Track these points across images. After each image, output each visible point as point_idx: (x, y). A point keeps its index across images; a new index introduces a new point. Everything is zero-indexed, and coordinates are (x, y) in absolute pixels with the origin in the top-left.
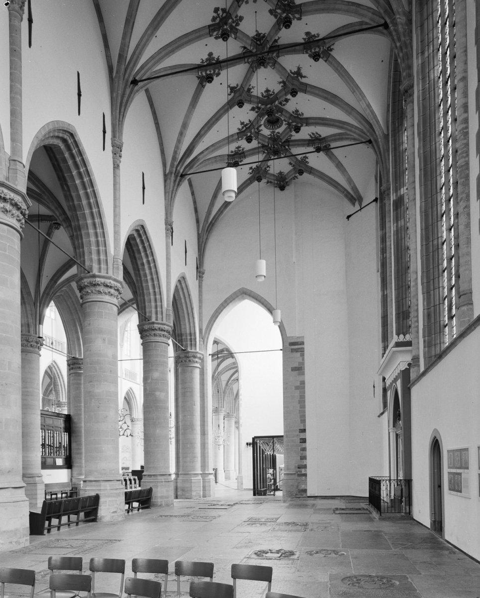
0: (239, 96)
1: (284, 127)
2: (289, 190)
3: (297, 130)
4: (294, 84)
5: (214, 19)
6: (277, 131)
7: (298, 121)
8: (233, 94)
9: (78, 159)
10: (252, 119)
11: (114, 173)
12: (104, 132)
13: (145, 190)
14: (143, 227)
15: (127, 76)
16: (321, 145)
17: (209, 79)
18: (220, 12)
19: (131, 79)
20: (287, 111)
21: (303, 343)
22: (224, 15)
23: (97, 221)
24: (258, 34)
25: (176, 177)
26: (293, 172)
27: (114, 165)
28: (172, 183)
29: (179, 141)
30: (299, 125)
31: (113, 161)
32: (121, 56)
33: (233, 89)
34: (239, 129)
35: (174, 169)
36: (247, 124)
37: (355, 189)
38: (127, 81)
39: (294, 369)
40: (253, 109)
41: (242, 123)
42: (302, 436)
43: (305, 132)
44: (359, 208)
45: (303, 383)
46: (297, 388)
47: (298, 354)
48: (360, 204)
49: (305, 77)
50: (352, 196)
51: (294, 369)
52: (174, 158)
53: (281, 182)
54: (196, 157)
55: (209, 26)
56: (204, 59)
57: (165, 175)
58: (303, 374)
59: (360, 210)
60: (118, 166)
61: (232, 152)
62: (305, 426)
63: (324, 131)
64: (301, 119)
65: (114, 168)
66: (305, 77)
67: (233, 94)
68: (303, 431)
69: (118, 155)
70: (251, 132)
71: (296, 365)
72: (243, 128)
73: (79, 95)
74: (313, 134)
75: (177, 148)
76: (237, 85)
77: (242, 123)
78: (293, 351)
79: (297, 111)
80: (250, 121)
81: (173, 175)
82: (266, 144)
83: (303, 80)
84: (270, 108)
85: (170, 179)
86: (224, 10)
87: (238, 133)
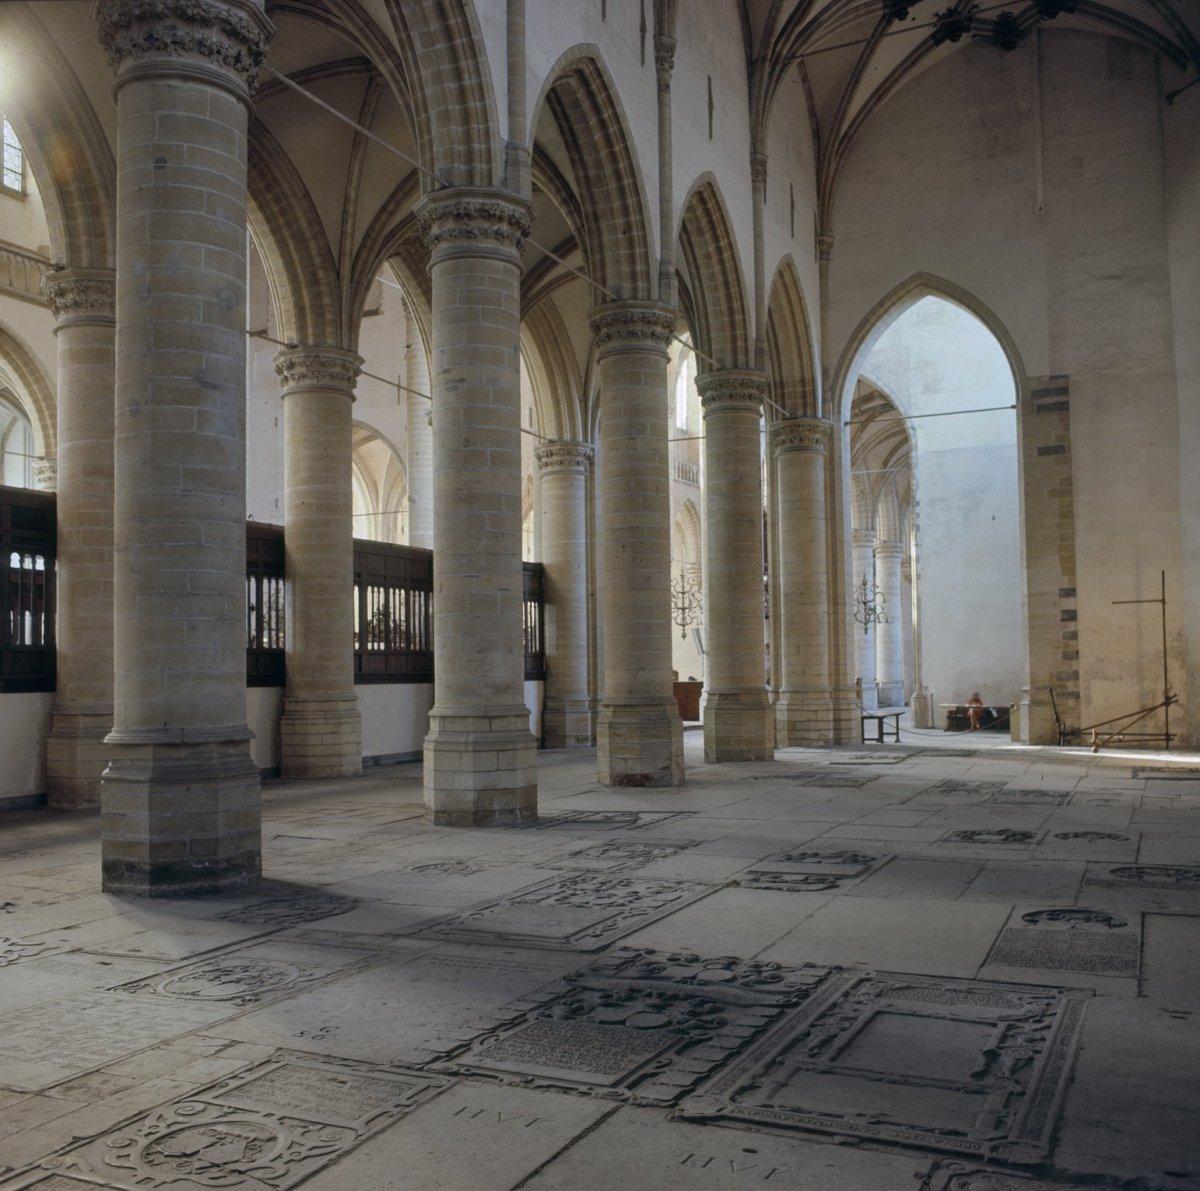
9: (600, 98)
13: (714, 111)
14: (710, 185)
21: (1064, 391)
23: (631, 201)
27: (659, 85)
39: (1044, 451)
42: (1068, 604)
45: (1069, 482)
46: (1053, 493)
47: (1054, 417)
51: (1044, 451)
54: (815, 19)
58: (1068, 462)
60: (668, 86)
62: (1073, 580)
68: (1070, 592)
71: (1052, 442)
78: (1041, 409)
85: (761, 72)
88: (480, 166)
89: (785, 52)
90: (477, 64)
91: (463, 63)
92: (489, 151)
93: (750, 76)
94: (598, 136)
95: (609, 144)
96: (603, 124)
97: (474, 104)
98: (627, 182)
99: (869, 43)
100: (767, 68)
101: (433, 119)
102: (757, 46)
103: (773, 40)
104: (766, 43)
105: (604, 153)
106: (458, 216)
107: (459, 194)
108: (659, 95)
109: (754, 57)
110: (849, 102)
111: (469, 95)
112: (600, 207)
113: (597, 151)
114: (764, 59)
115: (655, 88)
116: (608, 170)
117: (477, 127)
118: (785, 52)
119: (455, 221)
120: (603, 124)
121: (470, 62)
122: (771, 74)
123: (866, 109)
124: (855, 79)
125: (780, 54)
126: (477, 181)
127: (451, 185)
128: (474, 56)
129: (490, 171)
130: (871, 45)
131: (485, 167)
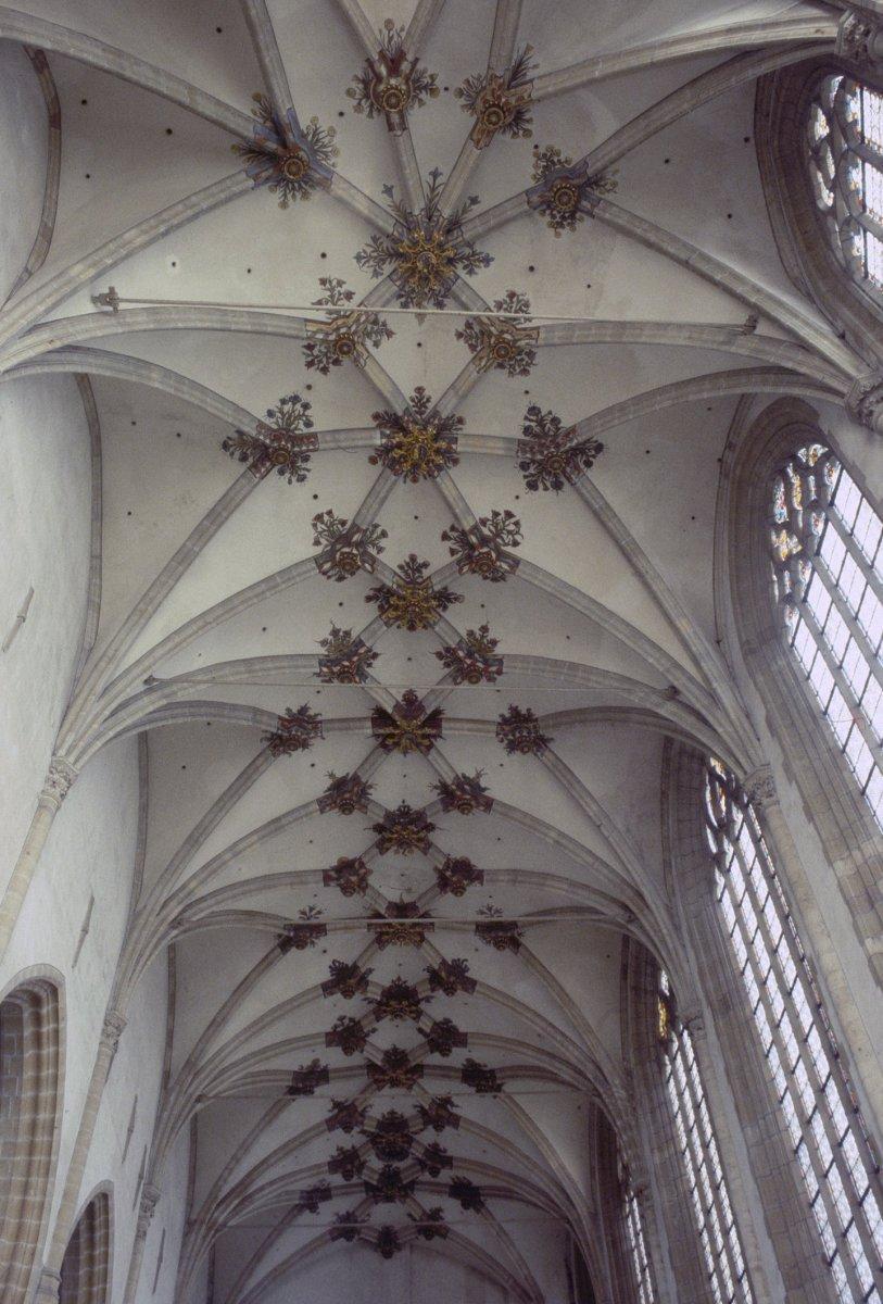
1: (409, 1161)
2: (400, 1257)
3: (435, 1173)
5: (336, 1026)
7: (436, 1158)
8: (336, 1111)
9: (99, 1234)
12: (141, 1177)
15: (194, 1086)
16: (468, 1195)
17: (308, 1091)
18: (346, 1021)
19: (198, 1093)
22: (352, 1024)
26: (413, 1230)
27: (139, 1231)
29: (229, 1169)
30: (439, 1166)
31: (139, 1225)
32: (189, 1064)
33: (337, 1105)
34: (332, 1157)
35: (209, 1216)
36: (348, 1151)
40: (363, 1132)
43: (446, 1176)
49: (457, 1106)
52: (212, 1195)
53: (387, 1243)
55: (327, 1034)
56: (305, 1066)
61: (310, 1186)
63: (477, 1179)
64: (440, 1156)
65: (137, 1236)
66: (457, 1106)
67: (336, 1111)
70: (353, 1166)
72: (339, 1155)
74: (457, 1177)
75: (222, 1179)
76: (346, 1101)
80: (353, 1147)
81: (204, 1227)
82: (375, 1183)
83: (454, 1110)
86: (351, 1020)
87: (329, 1163)
89: (221, 1220)
90: (46, 1183)
91: (33, 1179)
92: (29, 1272)
93: (186, 1235)
95: (90, 1282)
97: (30, 1221)
99: (275, 1229)
100: (203, 1231)
102: (197, 1208)
108: (136, 1240)
109: (194, 1217)
113: (76, 1285)
117: (26, 1245)
121: (41, 1180)
122: (204, 1237)
124: (258, 1257)
125: (216, 1222)
130: (278, 1231)
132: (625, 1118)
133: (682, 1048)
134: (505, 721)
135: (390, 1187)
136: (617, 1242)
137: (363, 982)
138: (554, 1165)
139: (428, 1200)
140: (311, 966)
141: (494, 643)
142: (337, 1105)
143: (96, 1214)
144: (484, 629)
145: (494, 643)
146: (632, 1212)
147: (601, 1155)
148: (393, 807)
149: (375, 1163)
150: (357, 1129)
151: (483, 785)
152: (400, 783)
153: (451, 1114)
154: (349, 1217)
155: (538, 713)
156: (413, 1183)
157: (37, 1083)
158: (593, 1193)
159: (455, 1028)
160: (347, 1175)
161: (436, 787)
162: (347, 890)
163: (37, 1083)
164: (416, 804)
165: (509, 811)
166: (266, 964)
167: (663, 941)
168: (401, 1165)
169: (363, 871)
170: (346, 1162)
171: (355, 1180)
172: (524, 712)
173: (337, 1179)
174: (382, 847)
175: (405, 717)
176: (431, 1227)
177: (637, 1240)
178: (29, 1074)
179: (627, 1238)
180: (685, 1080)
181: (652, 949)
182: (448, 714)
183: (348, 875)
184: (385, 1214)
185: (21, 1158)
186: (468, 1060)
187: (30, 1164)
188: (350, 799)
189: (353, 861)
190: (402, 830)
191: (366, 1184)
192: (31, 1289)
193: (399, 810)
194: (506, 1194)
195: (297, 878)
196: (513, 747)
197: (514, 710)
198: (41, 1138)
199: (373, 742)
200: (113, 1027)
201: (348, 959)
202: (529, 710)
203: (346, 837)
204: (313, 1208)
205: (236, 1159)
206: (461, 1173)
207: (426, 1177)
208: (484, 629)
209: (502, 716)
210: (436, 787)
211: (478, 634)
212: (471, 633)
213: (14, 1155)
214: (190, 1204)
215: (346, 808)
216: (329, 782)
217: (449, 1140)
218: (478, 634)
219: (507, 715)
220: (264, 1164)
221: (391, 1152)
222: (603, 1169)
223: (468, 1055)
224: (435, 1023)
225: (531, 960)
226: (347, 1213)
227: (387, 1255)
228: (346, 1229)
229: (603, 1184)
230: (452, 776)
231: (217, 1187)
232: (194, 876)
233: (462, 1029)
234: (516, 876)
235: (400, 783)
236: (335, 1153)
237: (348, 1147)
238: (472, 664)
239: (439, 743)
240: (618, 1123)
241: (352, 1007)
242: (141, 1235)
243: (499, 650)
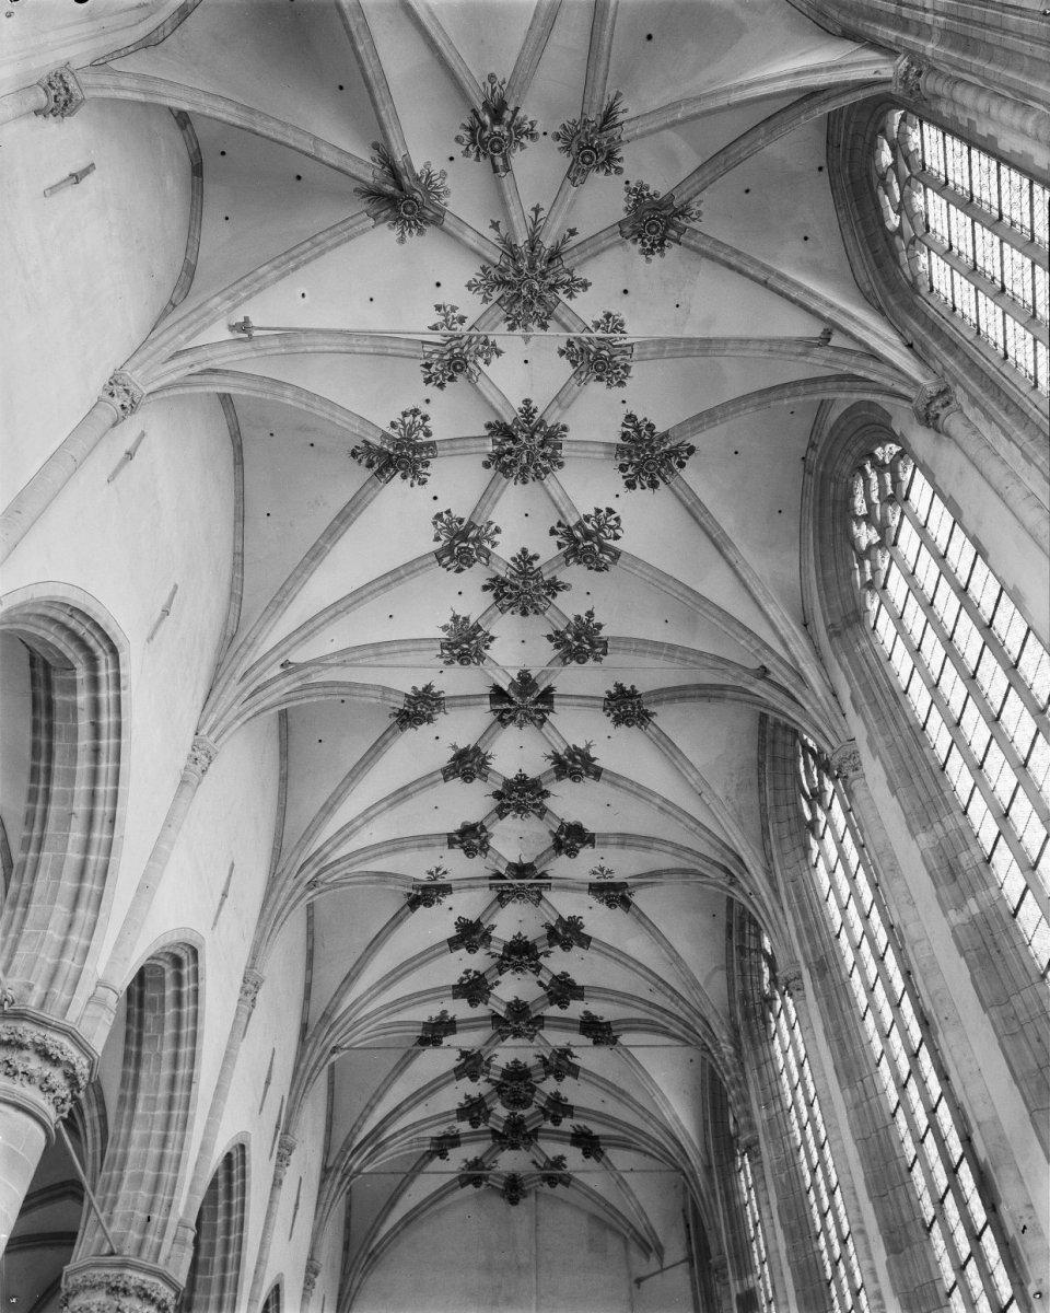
0: (471, 1065)
2: (527, 1203)
3: (557, 1122)
4: (561, 1065)
5: (462, 979)
6: (520, 1112)
7: (558, 1108)
9: (236, 1184)
10: (484, 1094)
11: (271, 1196)
12: (277, 1127)
16: (588, 1143)
17: (436, 1042)
18: (472, 974)
20: (542, 1093)
24: (517, 1001)
25: (345, 1175)
28: (334, 1189)
29: (363, 1118)
32: (326, 1016)
33: (464, 1054)
34: (461, 1104)
37: (651, 1230)
38: (325, 1048)
40: (489, 1080)
41: (467, 1097)
43: (567, 1125)
44: (658, 1268)
48: (661, 1259)
50: (644, 1241)
52: (347, 1144)
53: (513, 1189)
55: (454, 986)
57: (326, 1170)
59: (662, 1270)
60: (281, 1182)
63: (597, 1129)
65: (274, 1185)
69: (285, 1163)
73: (268, 1083)
75: (357, 1127)
77: (467, 1097)
79: (557, 1094)
81: (340, 1174)
82: (501, 1130)
83: (573, 1061)
84: (516, 1082)
86: (476, 973)
88: (152, 1239)
89: (355, 1167)
90: (183, 1137)
93: (322, 1181)
94: (220, 1221)
95: (228, 1232)
96: (229, 1208)
97: (167, 1174)
98: (230, 1274)
101: (126, 1178)
102: (333, 1156)
103: (349, 1153)
104: (342, 1154)
105: (219, 1240)
106: (115, 1289)
107: (124, 1265)
109: (330, 1164)
110: (381, 1224)
111: (167, 1164)
112: (197, 1296)
113: (214, 1235)
114: (337, 1170)
115: (270, 1181)
116: (217, 1258)
117: (162, 1196)
118: (355, 1167)
119: (108, 1293)
120: (229, 1208)
121: (178, 1133)
122: (341, 1183)
123: (395, 1232)
124: (392, 1203)
125: (351, 1167)
126: (145, 1255)
127: (120, 1253)
128: (184, 1127)
129: (159, 1246)
131: (156, 1240)
132: (733, 1074)
133: (784, 1006)
134: (611, 697)
135: (515, 1135)
136: (730, 1194)
137: (486, 938)
138: (668, 1117)
139: (552, 1149)
140: (436, 923)
141: (600, 626)
142: (464, 1054)
143: (234, 1163)
144: (590, 614)
145: (600, 626)
146: (744, 1165)
147: (714, 1108)
148: (511, 775)
149: (501, 1111)
150: (482, 1078)
151: (592, 755)
152: (517, 752)
153: (571, 1064)
154: (476, 1164)
155: (640, 690)
156: (536, 1130)
157: (177, 1039)
158: (705, 1144)
159: (572, 981)
160: (474, 1124)
161: (549, 757)
162: (470, 852)
163: (177, 1039)
164: (531, 774)
165: (616, 780)
166: (396, 920)
167: (763, 906)
168: (525, 1113)
169: (484, 835)
170: (473, 1110)
171: (482, 1127)
172: (628, 689)
173: (464, 1127)
174: (501, 812)
175: (520, 694)
176: (554, 1174)
177: (749, 1194)
178: (169, 1031)
179: (739, 1192)
180: (792, 1039)
181: (752, 910)
182: (558, 691)
183: (470, 838)
184: (510, 1161)
185: (160, 1112)
186: (585, 1012)
187: (169, 1118)
188: (471, 768)
189: (475, 825)
190: (520, 795)
191: (493, 1131)
192: (168, 1241)
193: (516, 778)
194: (625, 1145)
195: (424, 841)
196: (618, 721)
197: (619, 687)
198: (179, 1093)
199: (491, 717)
200: (251, 985)
201: (472, 916)
202: (633, 687)
203: (468, 802)
204: (443, 1155)
205: (370, 1107)
206: (582, 1123)
207: (549, 1125)
208: (590, 614)
209: (609, 692)
210: (549, 757)
211: (584, 618)
212: (578, 618)
213: (154, 1110)
214: (327, 1151)
215: (468, 777)
216: (452, 753)
217: (570, 1090)
218: (584, 618)
219: (613, 692)
220: (397, 1112)
221: (516, 1101)
222: (715, 1122)
223: (587, 1008)
224: (554, 976)
225: (641, 918)
226: (475, 1159)
227: (514, 1201)
228: (474, 1175)
229: (716, 1137)
230: (565, 748)
231: (352, 1135)
232: (328, 842)
233: (579, 983)
234: (625, 840)
235: (517, 752)
236: (463, 1101)
237: (474, 1095)
238: (579, 646)
239: (551, 717)
240: (727, 1078)
241: (478, 961)
242: (277, 1183)
243: (603, 633)
